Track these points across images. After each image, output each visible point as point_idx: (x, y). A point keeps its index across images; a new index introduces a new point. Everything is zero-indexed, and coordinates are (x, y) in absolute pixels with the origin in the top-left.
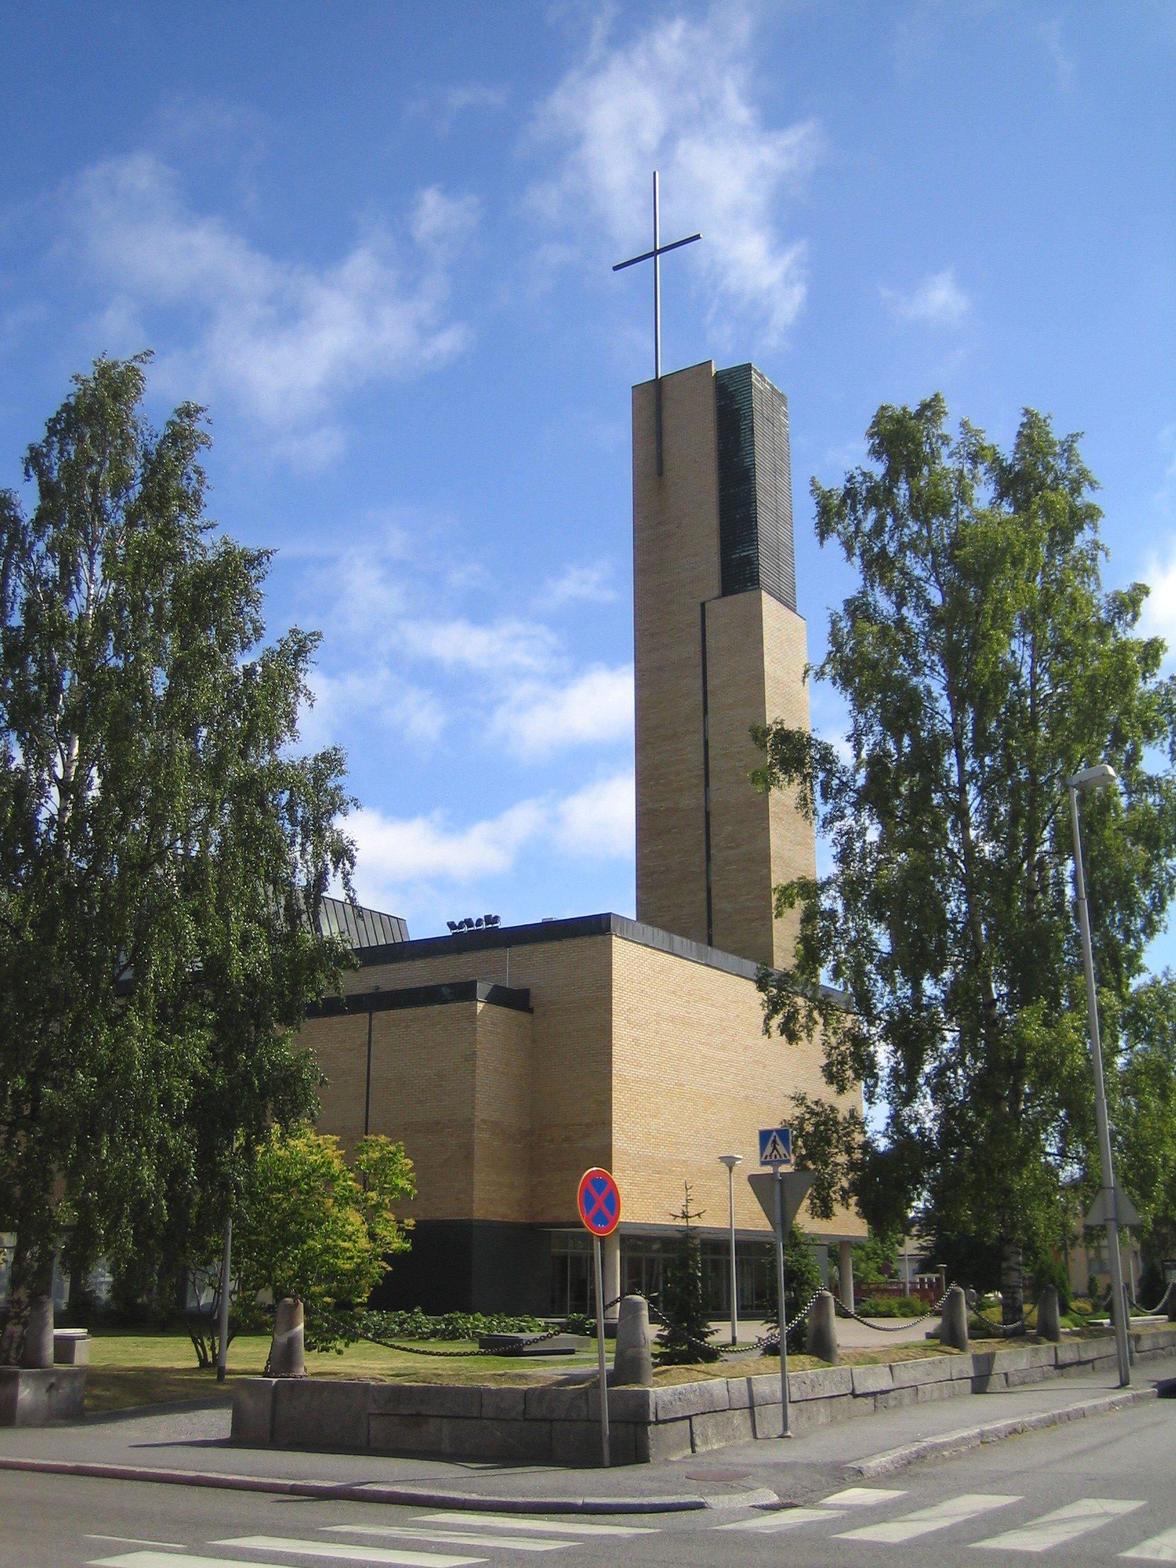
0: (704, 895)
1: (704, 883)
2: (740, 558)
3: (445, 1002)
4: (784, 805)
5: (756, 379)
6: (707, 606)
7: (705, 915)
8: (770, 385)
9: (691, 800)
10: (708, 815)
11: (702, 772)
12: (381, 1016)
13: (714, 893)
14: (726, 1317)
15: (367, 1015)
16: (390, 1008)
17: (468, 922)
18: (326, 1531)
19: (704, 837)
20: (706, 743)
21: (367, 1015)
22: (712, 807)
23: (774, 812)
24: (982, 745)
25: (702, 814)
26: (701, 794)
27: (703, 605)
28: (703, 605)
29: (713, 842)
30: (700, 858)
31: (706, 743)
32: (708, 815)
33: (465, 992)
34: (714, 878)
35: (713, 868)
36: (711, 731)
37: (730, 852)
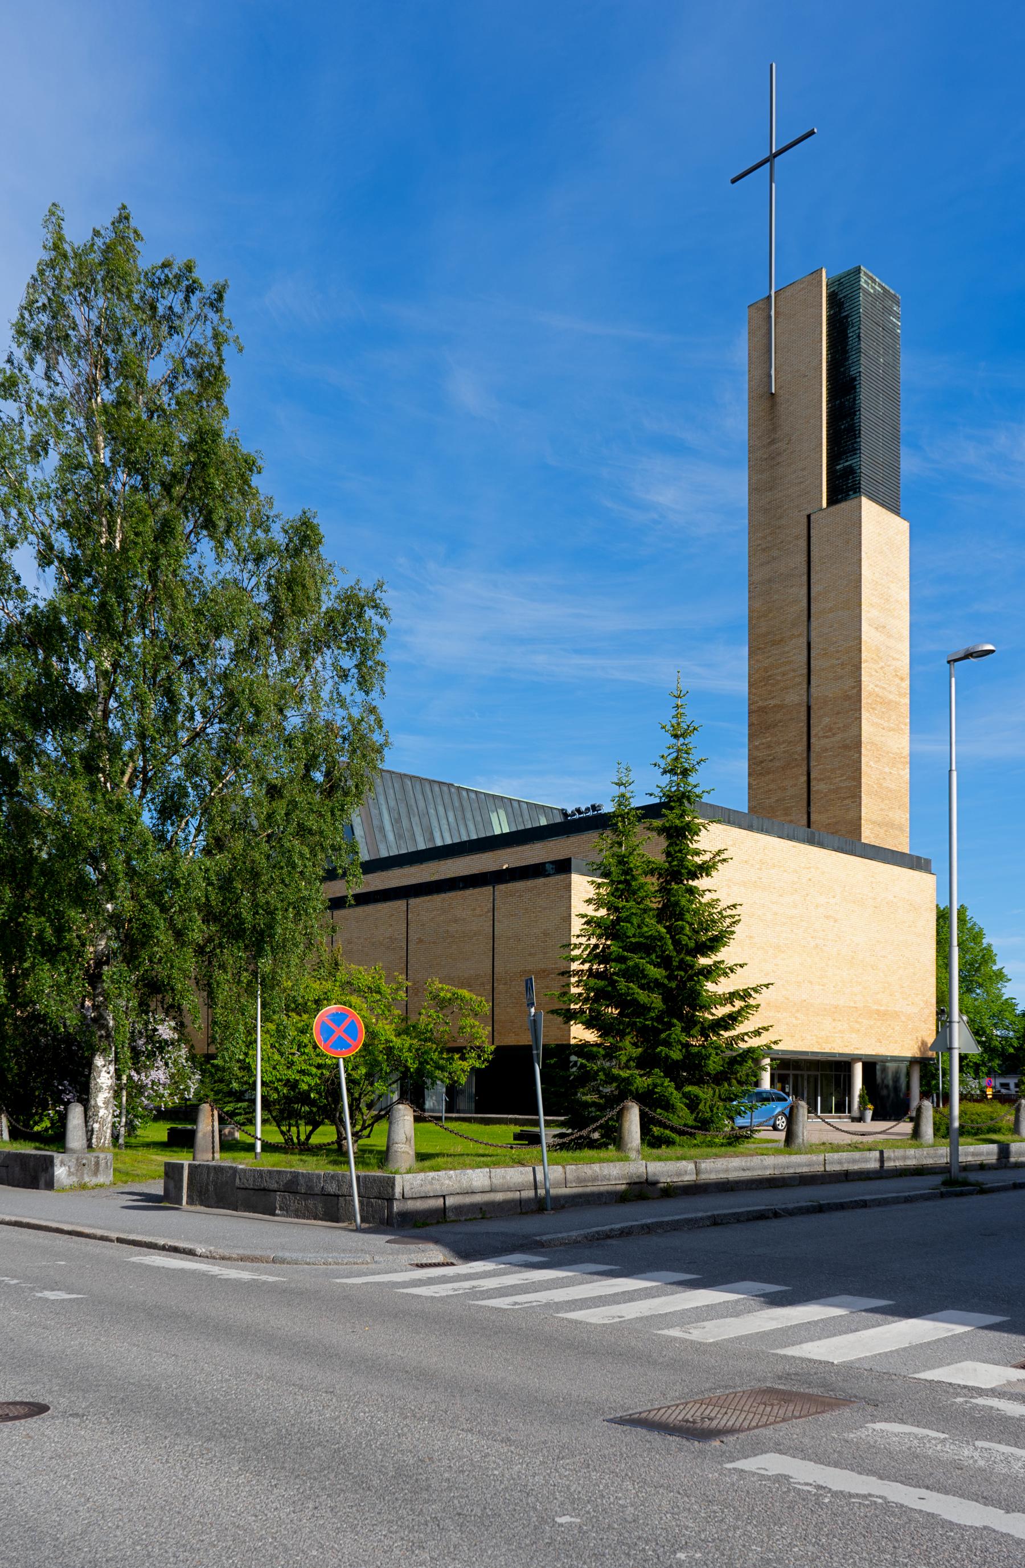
0: (805, 778)
1: (805, 768)
2: (845, 468)
3: (548, 875)
4: (877, 695)
5: (866, 282)
6: (812, 517)
7: (805, 796)
8: (880, 285)
9: (795, 697)
10: (809, 708)
11: (805, 671)
12: (501, 888)
13: (812, 776)
14: (391, 1183)
15: (491, 888)
16: (507, 882)
17: (579, 811)
18: (278, 1275)
19: (805, 729)
20: (809, 644)
21: (491, 888)
22: (812, 703)
23: (867, 703)
24: (31, 850)
25: (804, 709)
26: (804, 692)
27: (809, 516)
28: (809, 516)
29: (813, 733)
30: (802, 747)
31: (809, 644)
32: (809, 708)
33: (564, 867)
34: (813, 763)
35: (813, 755)
36: (813, 634)
37: (827, 740)
